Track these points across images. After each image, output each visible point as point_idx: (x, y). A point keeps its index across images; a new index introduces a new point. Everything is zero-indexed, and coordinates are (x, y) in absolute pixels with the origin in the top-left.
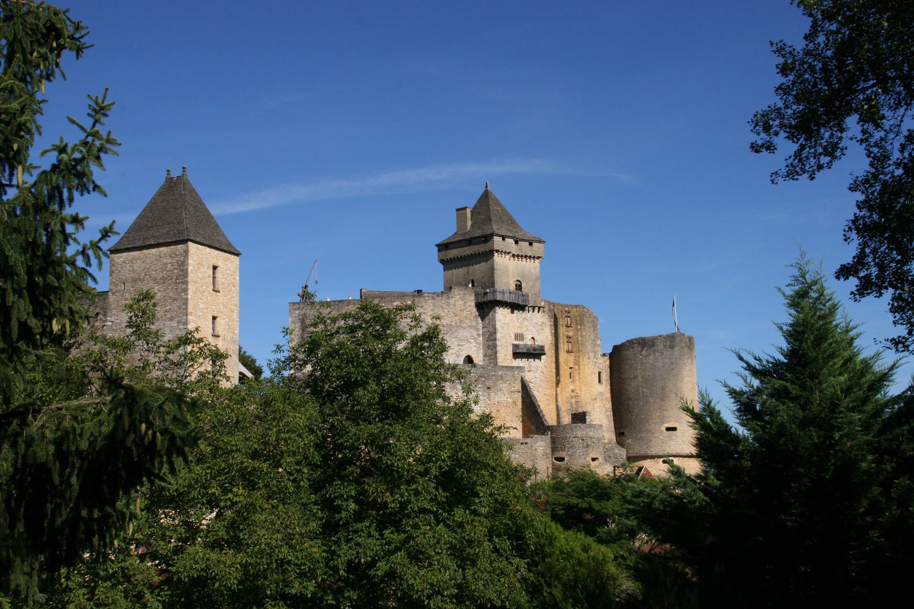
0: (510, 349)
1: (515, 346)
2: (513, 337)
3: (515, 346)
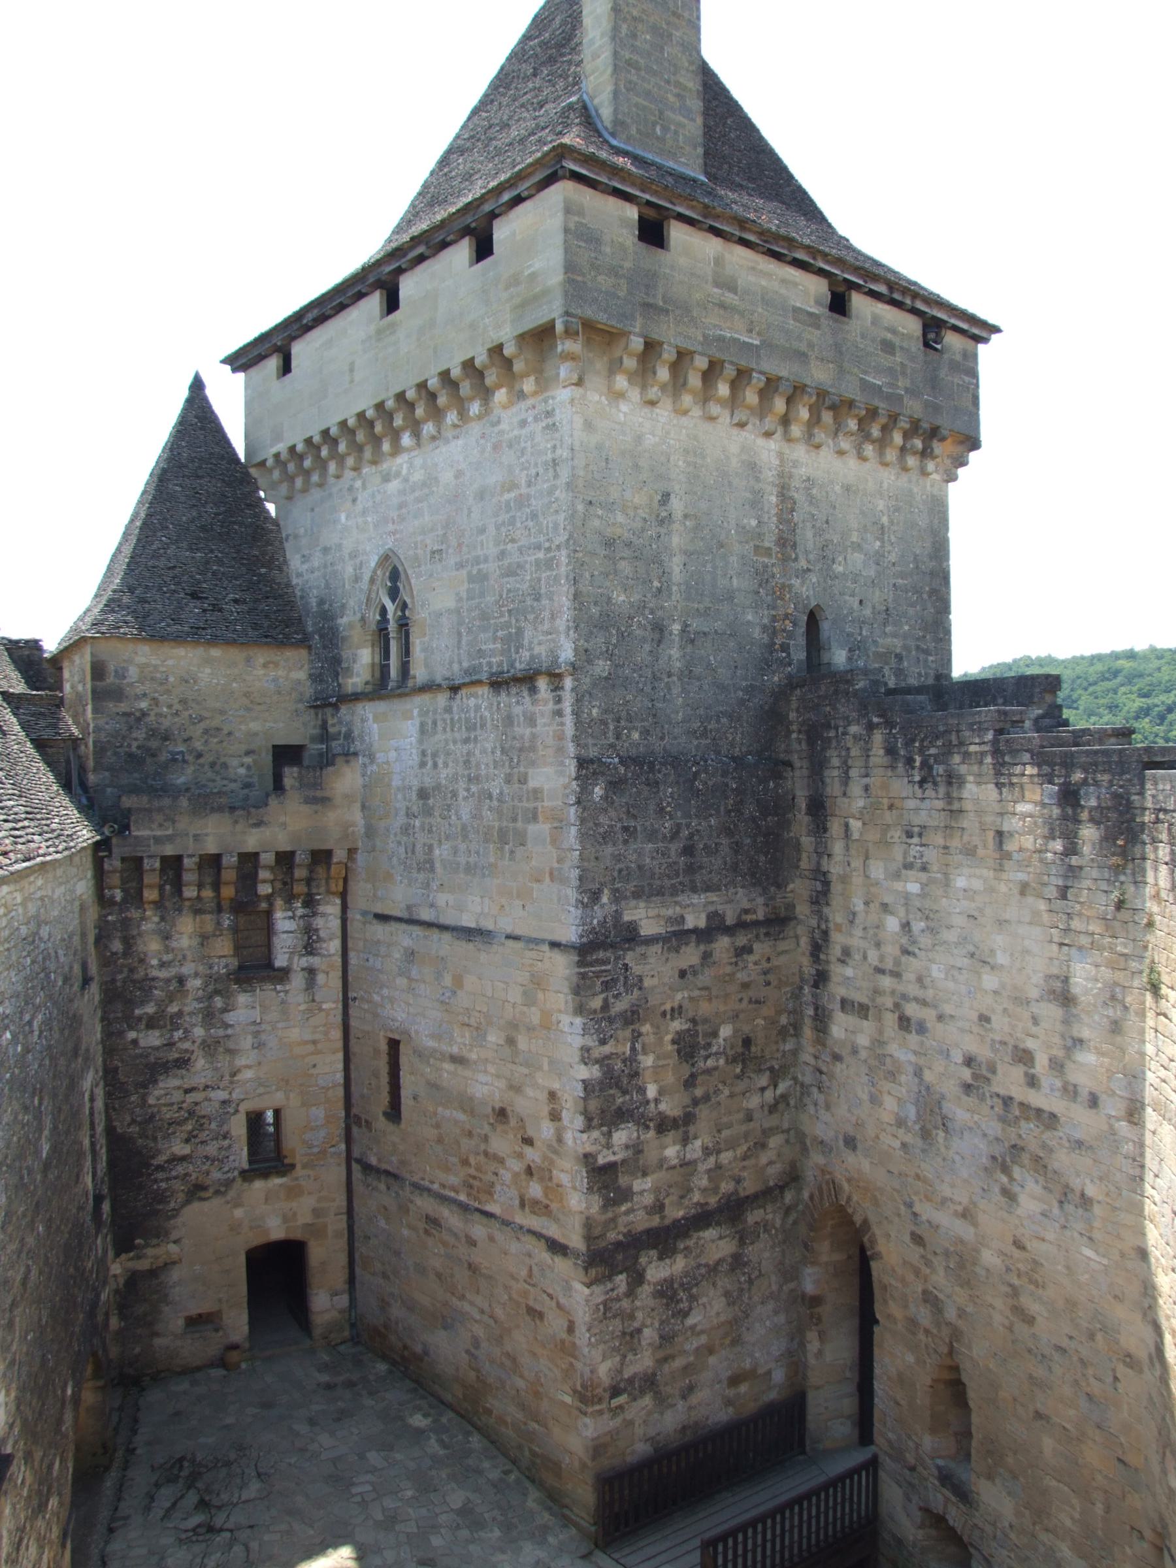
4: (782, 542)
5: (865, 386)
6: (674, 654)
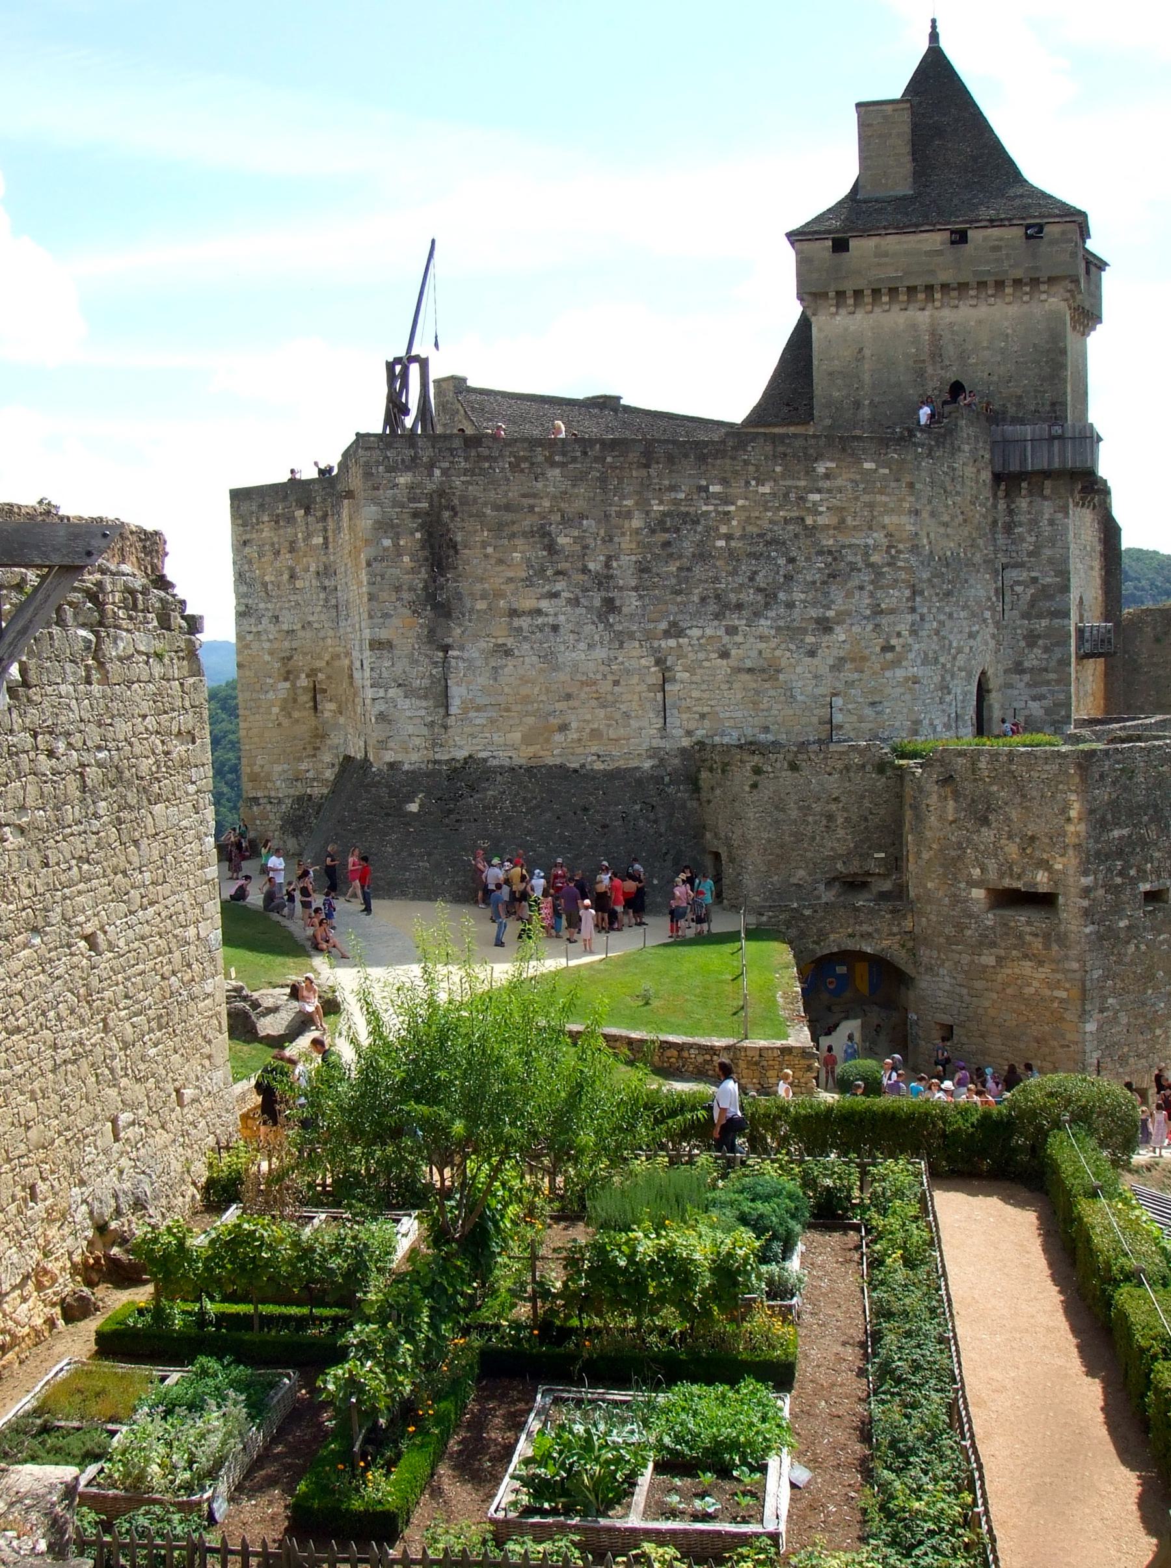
4: (933, 356)
5: (975, 273)
6: (866, 413)
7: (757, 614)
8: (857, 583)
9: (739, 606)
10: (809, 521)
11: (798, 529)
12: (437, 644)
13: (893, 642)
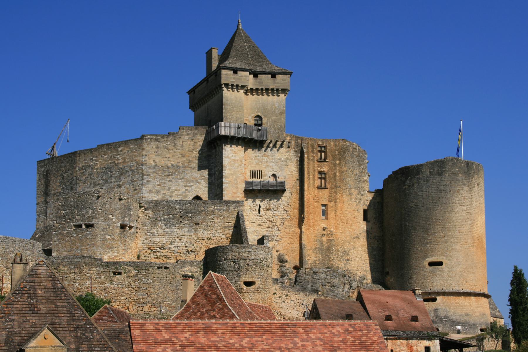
0: (242, 187)
1: (248, 183)
2: (248, 174)
3: (248, 183)
7: (103, 186)
8: (128, 175)
9: (99, 184)
10: (116, 162)
11: (114, 164)
12: (46, 202)
13: (137, 188)
